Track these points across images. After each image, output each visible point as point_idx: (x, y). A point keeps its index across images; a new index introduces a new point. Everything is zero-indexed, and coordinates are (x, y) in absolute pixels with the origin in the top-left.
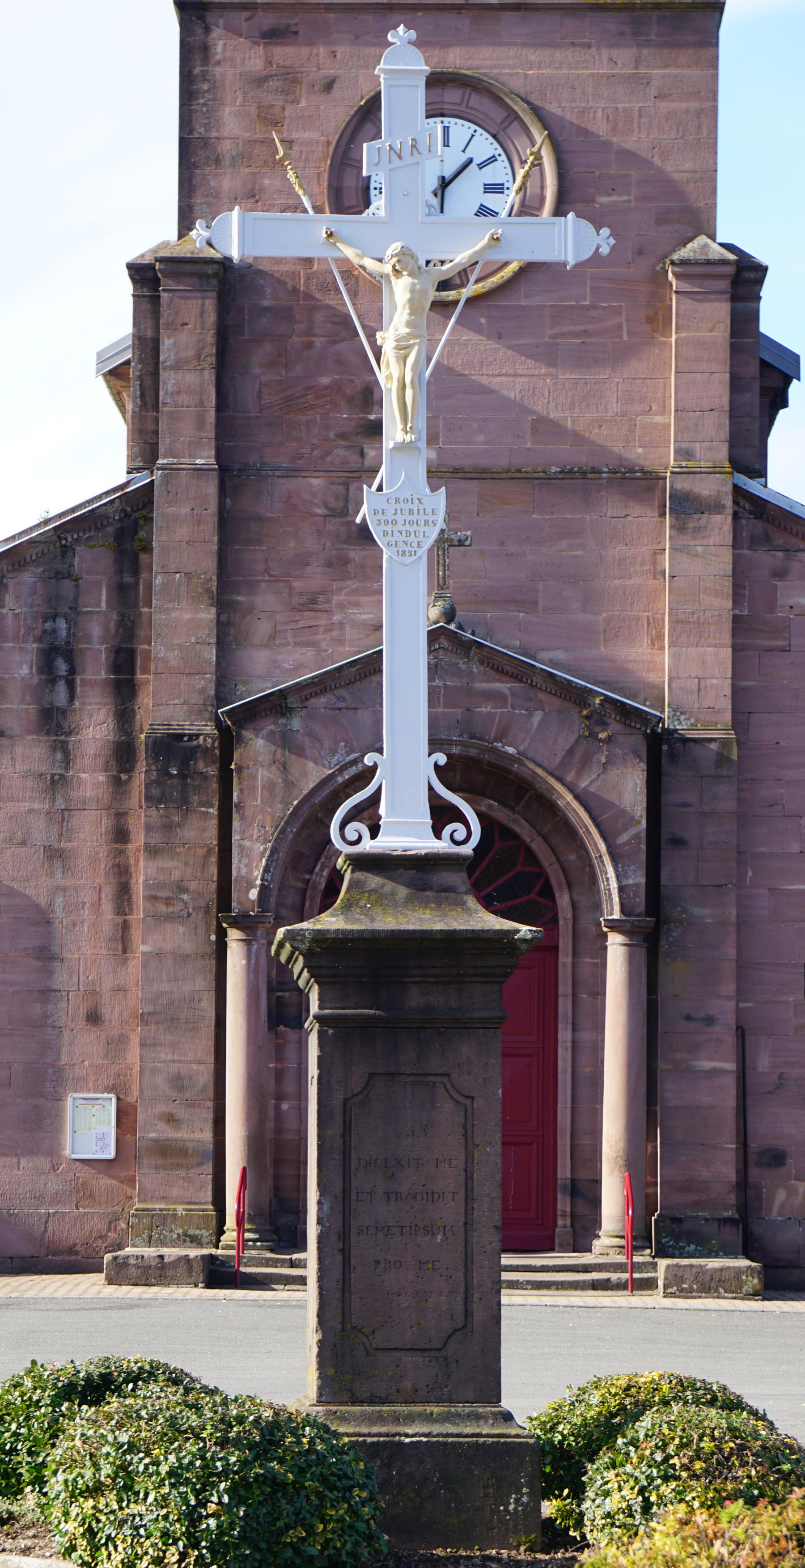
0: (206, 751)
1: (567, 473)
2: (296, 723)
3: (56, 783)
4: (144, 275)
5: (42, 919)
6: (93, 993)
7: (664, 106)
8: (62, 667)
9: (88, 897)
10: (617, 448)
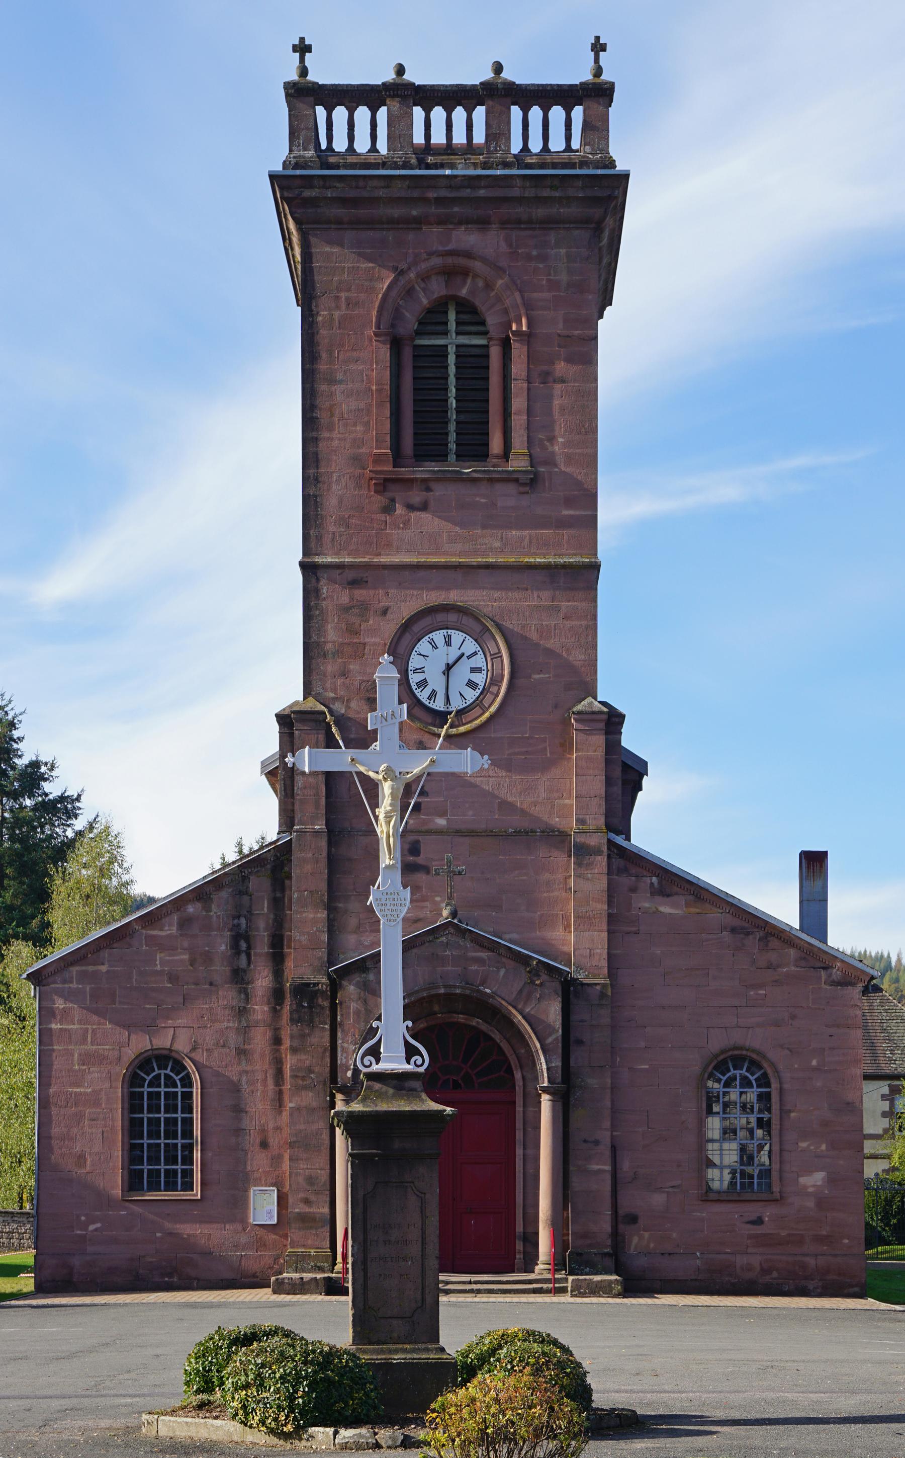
0: (323, 993)
1: (518, 833)
3: (241, 1012)
4: (285, 720)
5: (235, 1088)
6: (263, 1131)
7: (568, 623)
8: (243, 945)
9: (259, 1076)
10: (545, 818)
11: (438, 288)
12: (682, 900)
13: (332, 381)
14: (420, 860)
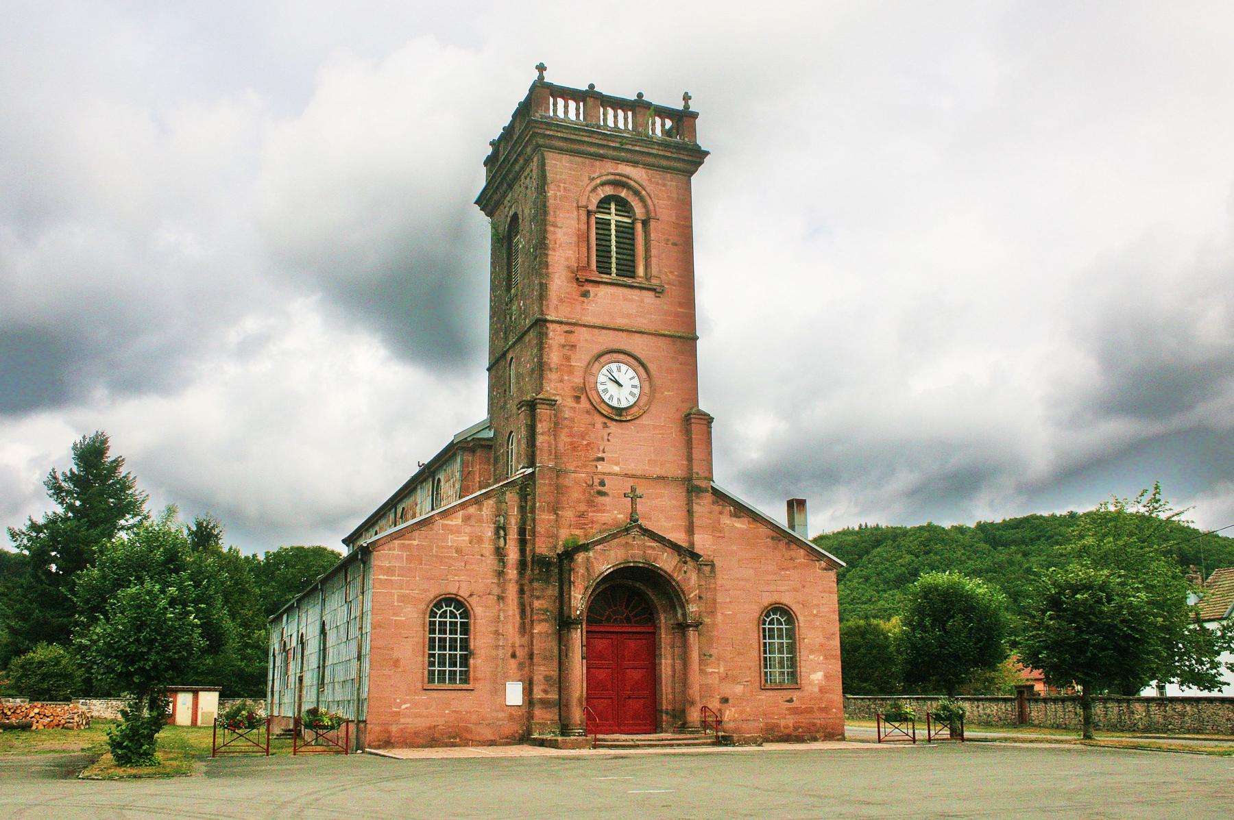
1: (659, 478)
2: (591, 554)
3: (500, 574)
8: (502, 533)
11: (609, 190)
12: (746, 520)
13: (555, 226)
14: (604, 489)
